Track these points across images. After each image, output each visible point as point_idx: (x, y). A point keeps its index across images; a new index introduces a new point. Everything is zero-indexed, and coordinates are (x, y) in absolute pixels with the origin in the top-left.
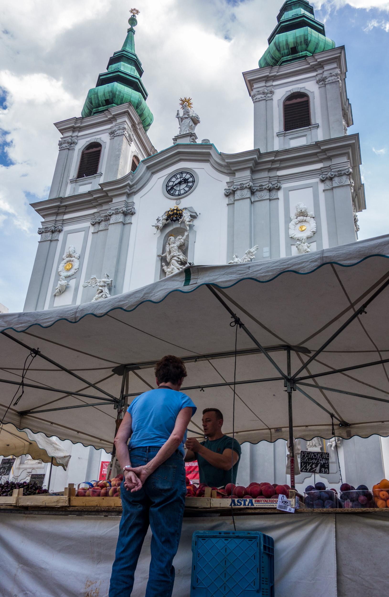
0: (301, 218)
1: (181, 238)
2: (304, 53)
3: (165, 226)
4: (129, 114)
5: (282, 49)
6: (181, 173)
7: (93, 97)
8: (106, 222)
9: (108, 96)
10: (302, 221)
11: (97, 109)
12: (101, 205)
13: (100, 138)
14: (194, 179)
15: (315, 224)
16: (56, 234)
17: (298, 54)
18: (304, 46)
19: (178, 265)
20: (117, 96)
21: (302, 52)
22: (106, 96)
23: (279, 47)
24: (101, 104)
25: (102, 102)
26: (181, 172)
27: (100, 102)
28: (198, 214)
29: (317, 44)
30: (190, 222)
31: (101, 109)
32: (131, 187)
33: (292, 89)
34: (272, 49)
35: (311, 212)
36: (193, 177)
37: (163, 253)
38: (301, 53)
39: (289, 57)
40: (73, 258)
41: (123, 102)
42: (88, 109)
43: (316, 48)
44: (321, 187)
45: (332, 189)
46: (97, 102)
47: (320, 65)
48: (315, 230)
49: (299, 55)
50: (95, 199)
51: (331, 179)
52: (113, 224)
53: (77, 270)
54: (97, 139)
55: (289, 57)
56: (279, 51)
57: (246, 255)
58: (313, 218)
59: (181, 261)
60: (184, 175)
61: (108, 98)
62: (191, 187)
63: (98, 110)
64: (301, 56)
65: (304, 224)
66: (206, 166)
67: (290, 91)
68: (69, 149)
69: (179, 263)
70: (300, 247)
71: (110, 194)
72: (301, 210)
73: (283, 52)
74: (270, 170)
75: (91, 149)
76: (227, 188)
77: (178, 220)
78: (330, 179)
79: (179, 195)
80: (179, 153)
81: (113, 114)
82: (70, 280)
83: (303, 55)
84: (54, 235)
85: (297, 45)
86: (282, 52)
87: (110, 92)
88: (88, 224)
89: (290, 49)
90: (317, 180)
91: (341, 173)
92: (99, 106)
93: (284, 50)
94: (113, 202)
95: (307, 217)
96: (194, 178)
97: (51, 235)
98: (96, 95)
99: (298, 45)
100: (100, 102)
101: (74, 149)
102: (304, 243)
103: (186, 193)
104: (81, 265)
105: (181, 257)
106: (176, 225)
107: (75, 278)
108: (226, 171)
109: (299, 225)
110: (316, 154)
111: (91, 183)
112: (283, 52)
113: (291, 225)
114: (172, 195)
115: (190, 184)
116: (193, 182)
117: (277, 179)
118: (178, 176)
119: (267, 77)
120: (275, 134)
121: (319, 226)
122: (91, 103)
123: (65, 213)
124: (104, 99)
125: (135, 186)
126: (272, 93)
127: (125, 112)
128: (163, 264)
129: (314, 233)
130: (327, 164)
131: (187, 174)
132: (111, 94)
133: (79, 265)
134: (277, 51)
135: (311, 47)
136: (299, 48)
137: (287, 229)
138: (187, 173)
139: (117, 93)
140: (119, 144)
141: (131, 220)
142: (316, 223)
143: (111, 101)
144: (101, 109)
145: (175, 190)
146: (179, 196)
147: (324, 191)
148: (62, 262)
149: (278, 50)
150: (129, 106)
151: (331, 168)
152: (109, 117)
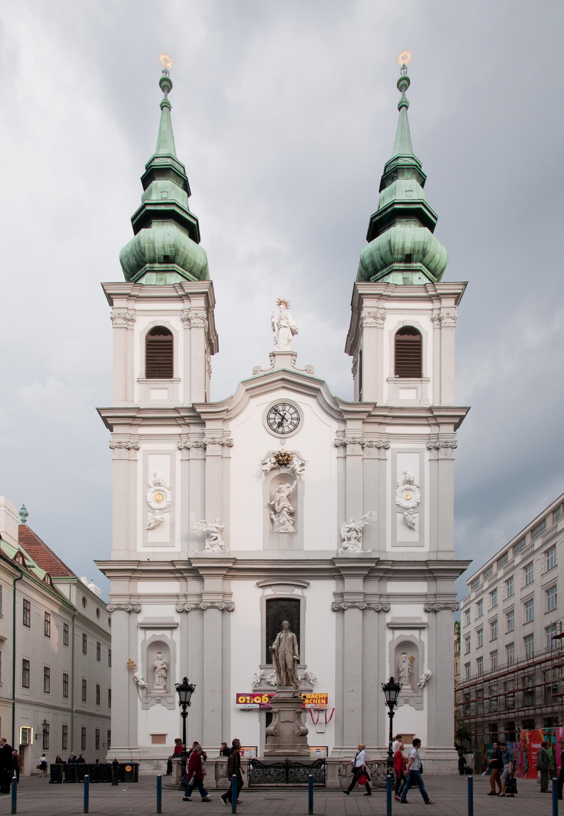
0: (408, 486)
1: (289, 485)
2: (418, 265)
3: (272, 469)
5: (396, 253)
6: (284, 405)
8: (197, 449)
9: (169, 252)
10: (408, 490)
11: (152, 265)
12: (187, 424)
15: (419, 495)
18: (420, 256)
20: (180, 254)
21: (416, 263)
22: (166, 251)
23: (394, 250)
24: (157, 259)
25: (159, 257)
26: (284, 403)
27: (157, 256)
29: (434, 256)
30: (300, 471)
31: (157, 266)
32: (227, 411)
34: (385, 247)
35: (417, 482)
37: (271, 501)
38: (415, 265)
40: (163, 488)
41: (187, 262)
42: (136, 260)
43: (431, 261)
44: (428, 455)
45: (438, 460)
46: (152, 255)
48: (419, 502)
49: (413, 267)
50: (182, 418)
51: (438, 449)
52: (212, 456)
53: (170, 503)
54: (165, 322)
55: (402, 266)
57: (361, 521)
58: (418, 487)
60: (287, 408)
61: (169, 254)
63: (153, 268)
64: (415, 268)
65: (409, 492)
66: (312, 402)
68: (126, 328)
69: (289, 514)
70: (407, 518)
71: (203, 417)
72: (409, 479)
73: (397, 256)
74: (380, 424)
75: (157, 336)
76: (337, 438)
77: (286, 465)
78: (437, 448)
80: (283, 380)
81: (187, 291)
82: (164, 513)
83: (417, 268)
85: (413, 253)
86: (395, 256)
87: (172, 246)
88: (172, 446)
89: (405, 256)
90: (423, 446)
91: (447, 445)
92: (153, 261)
93: (398, 254)
94: (206, 428)
95: (412, 485)
96: (298, 414)
98: (151, 245)
99: (415, 253)
100: (157, 256)
101: (133, 330)
102: (411, 515)
103: (291, 432)
104: (173, 497)
105: (291, 508)
106: (284, 470)
107: (169, 512)
109: (405, 493)
110: (426, 418)
111: (167, 389)
113: (399, 490)
115: (295, 422)
116: (298, 419)
120: (385, 379)
121: (422, 498)
122: (144, 255)
124: (163, 253)
126: (383, 319)
128: (272, 512)
129: (418, 504)
130: (435, 430)
131: (290, 407)
132: (173, 249)
133: (171, 497)
134: (390, 253)
135: (427, 259)
136: (415, 257)
137: (394, 495)
138: (291, 406)
139: (181, 249)
141: (230, 455)
142: (420, 494)
143: (172, 259)
146: (283, 434)
147: (430, 460)
148: (149, 490)
149: (391, 253)
150: (210, 286)
151: (439, 437)
152: (181, 293)
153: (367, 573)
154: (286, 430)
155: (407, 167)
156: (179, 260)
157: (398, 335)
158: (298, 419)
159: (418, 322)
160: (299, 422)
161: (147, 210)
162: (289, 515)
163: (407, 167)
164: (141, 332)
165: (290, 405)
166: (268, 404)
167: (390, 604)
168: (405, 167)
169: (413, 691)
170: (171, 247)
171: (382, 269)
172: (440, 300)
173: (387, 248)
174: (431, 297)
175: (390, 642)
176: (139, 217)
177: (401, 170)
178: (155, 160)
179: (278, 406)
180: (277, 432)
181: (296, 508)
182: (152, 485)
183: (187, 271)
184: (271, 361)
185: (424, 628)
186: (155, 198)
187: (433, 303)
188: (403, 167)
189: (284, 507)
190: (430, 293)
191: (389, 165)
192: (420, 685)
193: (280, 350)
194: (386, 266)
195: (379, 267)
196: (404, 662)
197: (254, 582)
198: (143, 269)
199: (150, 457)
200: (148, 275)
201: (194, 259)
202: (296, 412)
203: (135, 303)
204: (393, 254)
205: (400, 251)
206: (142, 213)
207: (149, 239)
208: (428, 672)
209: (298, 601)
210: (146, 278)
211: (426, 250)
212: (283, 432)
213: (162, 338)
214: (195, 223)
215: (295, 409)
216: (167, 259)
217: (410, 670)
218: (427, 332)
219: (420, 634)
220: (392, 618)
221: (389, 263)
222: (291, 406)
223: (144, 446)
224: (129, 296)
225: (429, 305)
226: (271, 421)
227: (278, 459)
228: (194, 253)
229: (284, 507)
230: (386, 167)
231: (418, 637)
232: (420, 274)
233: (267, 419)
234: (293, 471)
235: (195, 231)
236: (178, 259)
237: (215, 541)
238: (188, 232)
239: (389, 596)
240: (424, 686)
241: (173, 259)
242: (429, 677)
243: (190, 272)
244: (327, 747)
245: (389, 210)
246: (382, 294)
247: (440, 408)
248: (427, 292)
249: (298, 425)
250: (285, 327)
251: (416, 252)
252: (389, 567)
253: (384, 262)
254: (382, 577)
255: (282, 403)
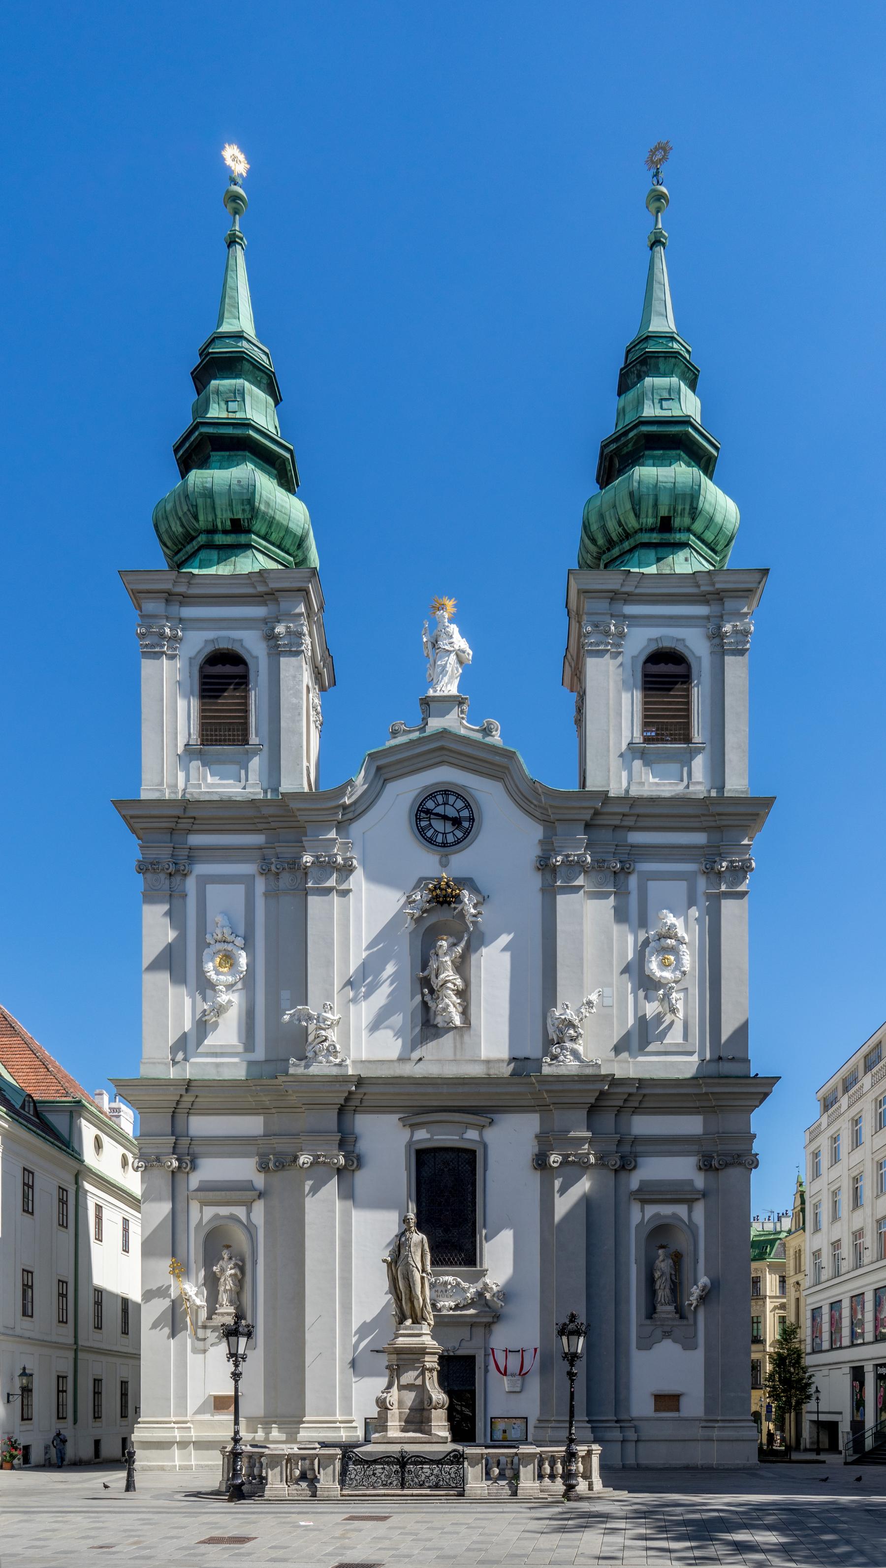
4: (307, 592)
5: (643, 515)
6: (445, 794)
7: (200, 502)
13: (241, 641)
14: (472, 813)
16: (178, 878)
17: (673, 535)
18: (687, 520)
19: (454, 998)
24: (219, 525)
25: (222, 522)
26: (445, 791)
28: (486, 897)
33: (660, 638)
36: (471, 808)
37: (423, 970)
39: (655, 538)
42: (183, 525)
44: (702, 883)
46: (210, 519)
47: (718, 594)
54: (234, 640)
55: (655, 538)
56: (637, 516)
59: (457, 990)
60: (452, 799)
62: (467, 832)
64: (677, 541)
67: (656, 640)
69: (455, 992)
73: (645, 520)
77: (449, 903)
79: (444, 845)
80: (442, 748)
84: (173, 879)
86: (643, 520)
87: (245, 503)
88: (248, 868)
96: (472, 810)
97: (167, 882)
99: (677, 514)
100: (219, 521)
103: (459, 843)
108: (537, 814)
112: (645, 520)
114: (431, 841)
116: (472, 819)
117: (628, 851)
118: (440, 799)
119: (615, 592)
122: (196, 517)
123: (190, 831)
124: (230, 515)
125: (352, 808)
126: (621, 635)
127: (299, 590)
128: (426, 991)
131: (457, 798)
134: (632, 515)
136: (677, 522)
140: (294, 677)
143: (246, 524)
144: (220, 539)
145: (435, 830)
149: (636, 515)
152: (261, 589)
153: (593, 1101)
154: (450, 839)
155: (663, 355)
156: (258, 526)
157: (649, 665)
158: (470, 819)
159: (683, 640)
160: (472, 825)
161: (201, 434)
162: (455, 995)
163: (663, 355)
164: (190, 658)
165: (456, 793)
166: (419, 790)
167: (636, 1156)
168: (660, 355)
169: (677, 1316)
170: (243, 504)
171: (622, 541)
172: (722, 600)
173: (628, 506)
174: (705, 596)
175: (637, 1226)
176: (187, 445)
177: (653, 361)
178: (216, 341)
179: (435, 796)
180: (433, 844)
181: (467, 982)
182: (212, 942)
183: (273, 544)
184: (423, 713)
185: (697, 1199)
186: (216, 412)
187: (710, 605)
188: (656, 355)
189: (446, 982)
190: (703, 588)
191: (633, 349)
192: (691, 1305)
193: (438, 694)
194: (627, 535)
195: (615, 538)
196: (663, 1261)
197: (396, 1117)
198: (194, 543)
199: (209, 887)
200: (203, 555)
201: (285, 523)
202: (468, 806)
203: (180, 606)
204: (639, 517)
205: (650, 511)
206: (192, 438)
207: (205, 488)
208: (703, 1280)
209: (473, 1152)
210: (200, 560)
211: (696, 508)
212: (444, 844)
213: (228, 669)
214: (288, 456)
215: (466, 800)
216: (237, 527)
217: (673, 1278)
218: (700, 658)
219: (690, 1211)
220: (641, 1181)
221: (634, 531)
222: (458, 796)
223: (201, 869)
224: (170, 597)
225: (701, 610)
226: (423, 824)
227: (434, 894)
228: (285, 514)
229: (446, 982)
230: (628, 352)
231: (686, 1220)
232: (686, 552)
233: (417, 819)
234: (462, 915)
235: (289, 468)
236: (255, 526)
237: (324, 1044)
238: (275, 472)
239: (636, 1140)
240: (696, 1308)
241: (249, 525)
242: (707, 1290)
243: (279, 547)
244: (526, 1418)
245: (631, 435)
246: (618, 590)
247: (721, 799)
248: (699, 586)
249: (471, 831)
250: (448, 651)
251: (679, 512)
252: (634, 1090)
253: (624, 529)
254: (621, 1107)
255: (442, 791)
